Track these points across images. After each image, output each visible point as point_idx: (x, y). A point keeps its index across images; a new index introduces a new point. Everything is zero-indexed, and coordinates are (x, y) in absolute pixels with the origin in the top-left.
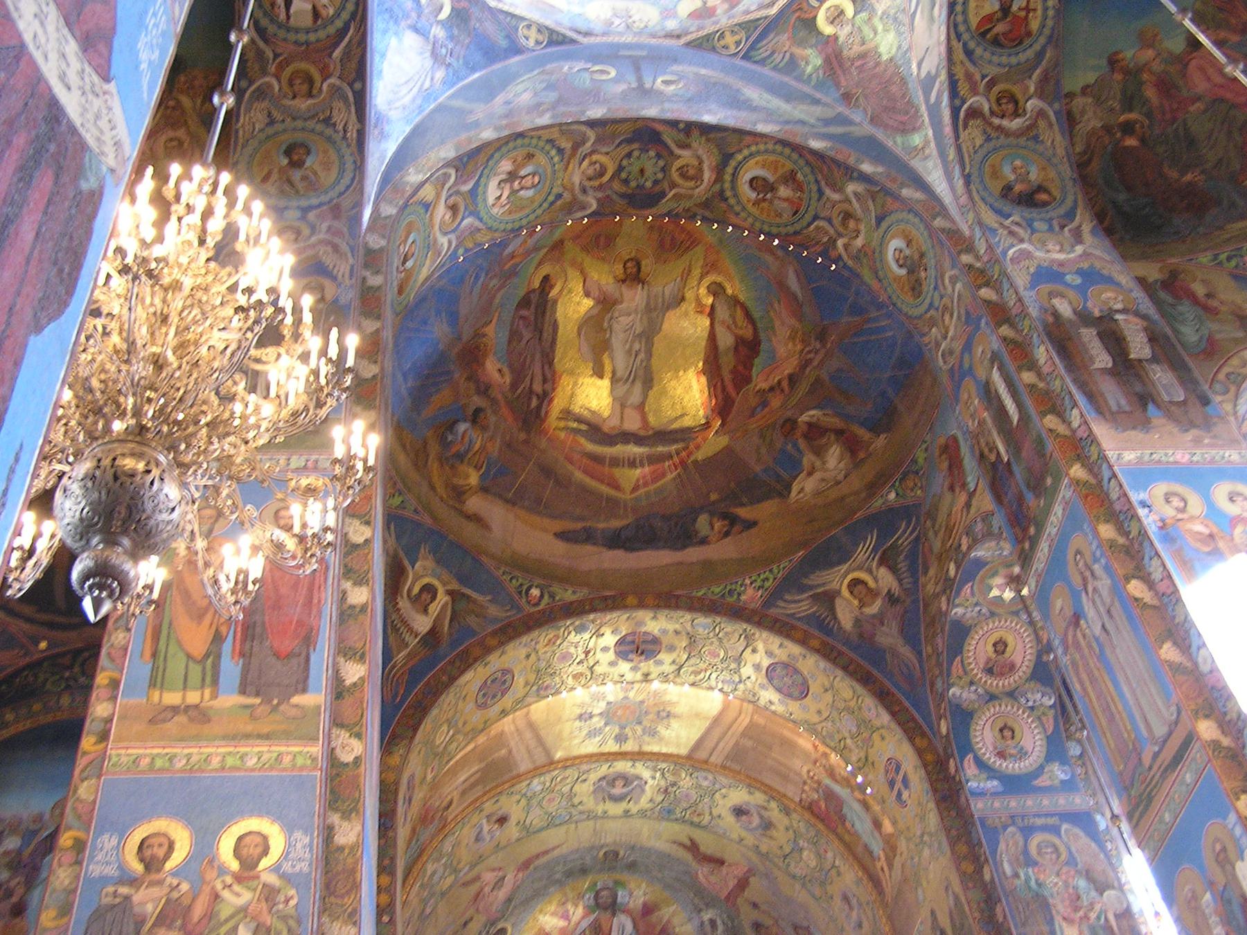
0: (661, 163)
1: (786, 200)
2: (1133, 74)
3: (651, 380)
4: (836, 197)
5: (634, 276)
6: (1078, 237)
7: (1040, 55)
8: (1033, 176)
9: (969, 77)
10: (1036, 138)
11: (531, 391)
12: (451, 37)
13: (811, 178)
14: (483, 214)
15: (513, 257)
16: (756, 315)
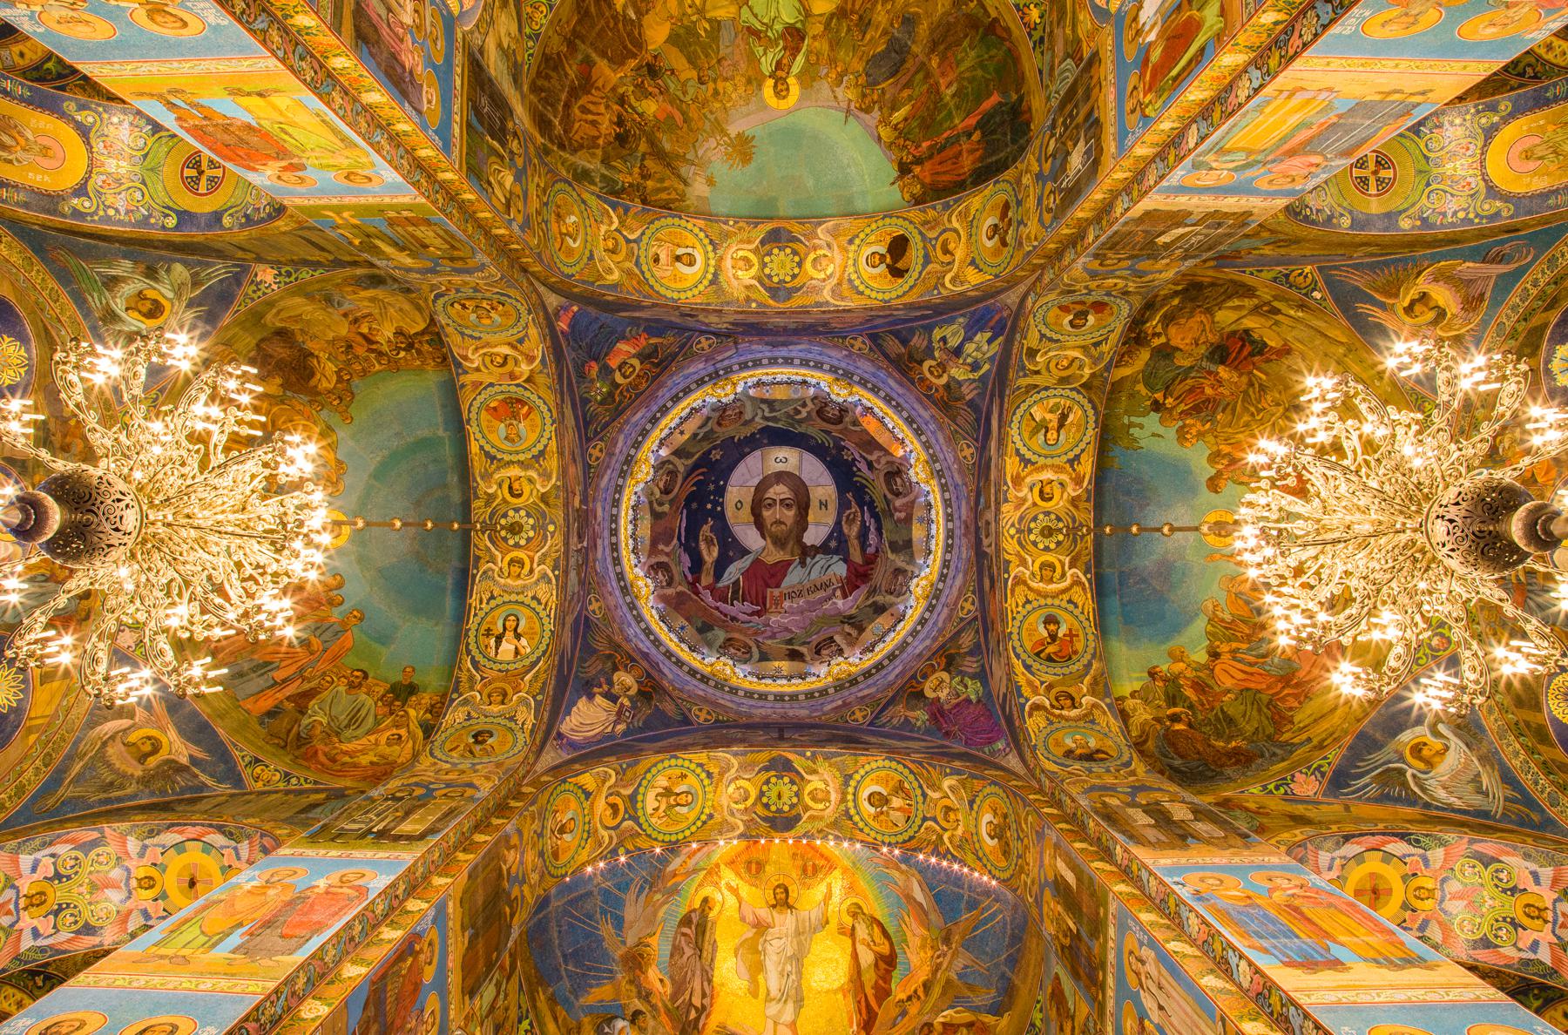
0: (795, 788)
1: (899, 809)
2: (1172, 681)
3: (802, 1000)
4: (936, 795)
5: (783, 901)
6: (1133, 773)
7: (1089, 666)
8: (1093, 743)
9: (1030, 683)
10: (1093, 722)
11: (691, 1004)
12: (634, 707)
13: (915, 784)
14: (642, 820)
15: (675, 875)
16: (891, 930)
